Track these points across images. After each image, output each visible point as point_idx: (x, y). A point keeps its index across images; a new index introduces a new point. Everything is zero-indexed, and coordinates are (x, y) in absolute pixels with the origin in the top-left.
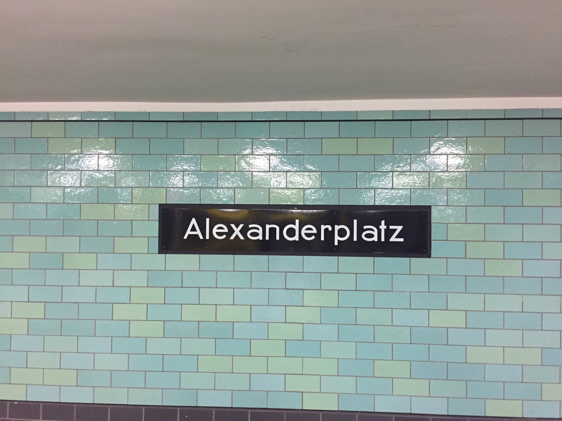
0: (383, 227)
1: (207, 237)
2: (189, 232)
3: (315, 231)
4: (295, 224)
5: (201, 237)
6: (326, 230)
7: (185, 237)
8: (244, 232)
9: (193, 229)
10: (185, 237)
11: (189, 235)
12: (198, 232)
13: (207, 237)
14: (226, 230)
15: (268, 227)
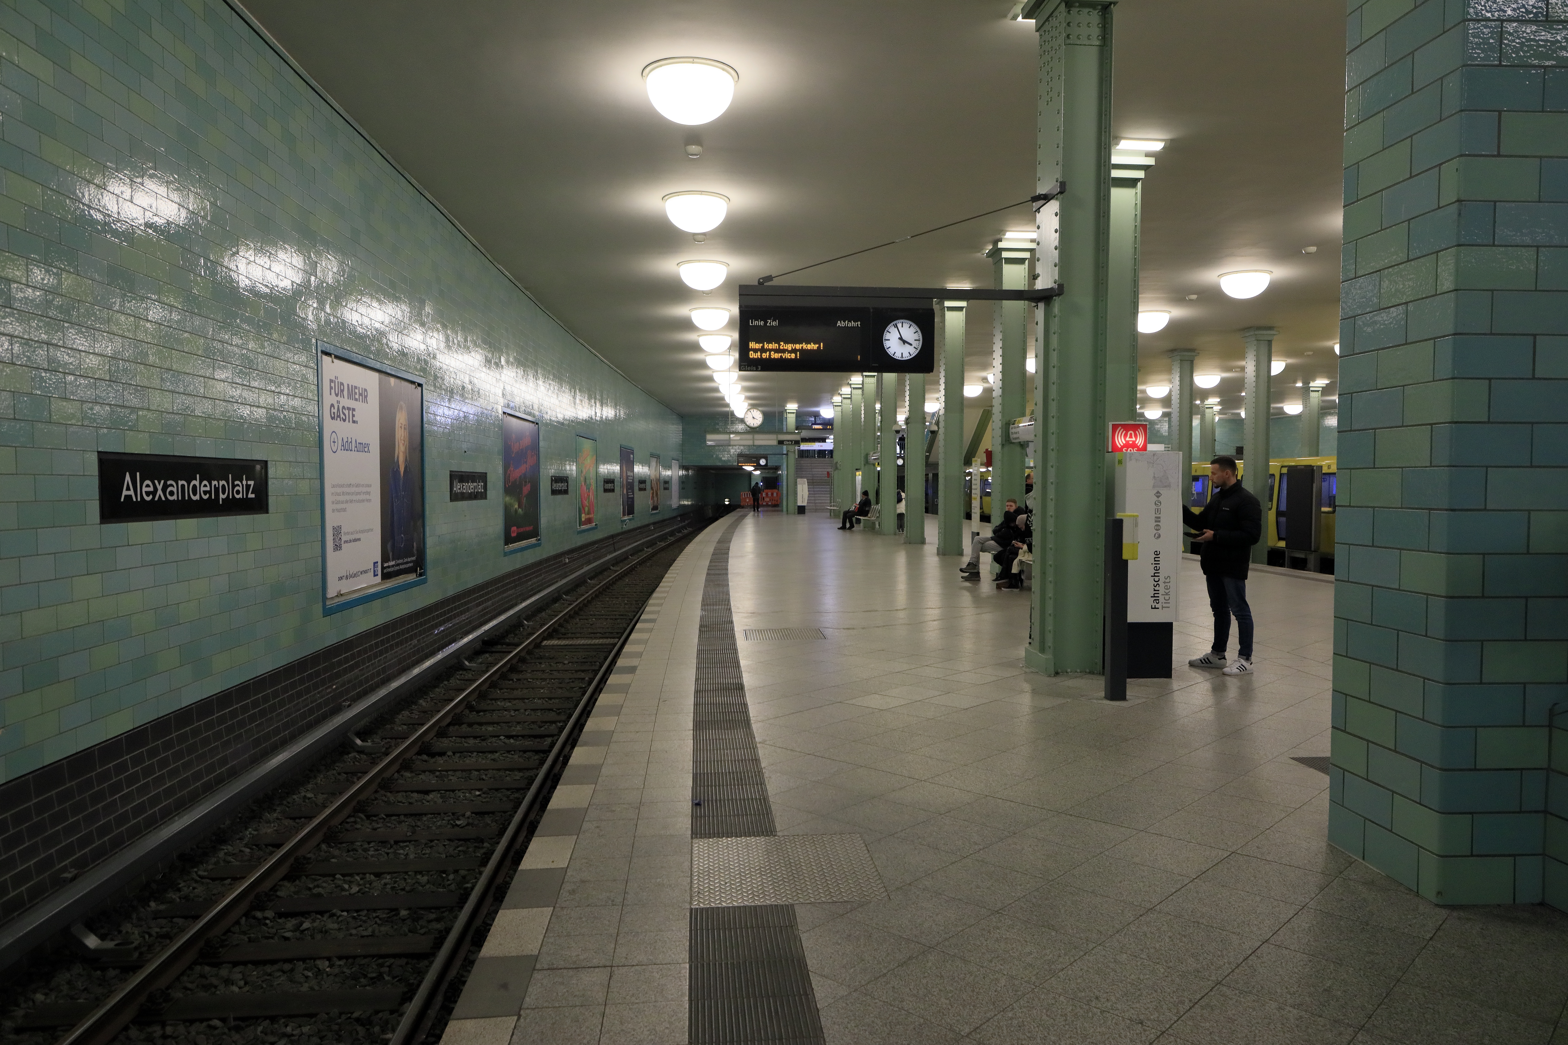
0: (244, 482)
1: (139, 499)
2: (125, 493)
3: (208, 489)
4: (196, 480)
5: (134, 499)
6: (215, 485)
7: (122, 500)
8: (164, 490)
9: (128, 489)
10: (122, 500)
11: (126, 496)
12: (131, 492)
13: (139, 499)
14: (151, 489)
15: (180, 483)
